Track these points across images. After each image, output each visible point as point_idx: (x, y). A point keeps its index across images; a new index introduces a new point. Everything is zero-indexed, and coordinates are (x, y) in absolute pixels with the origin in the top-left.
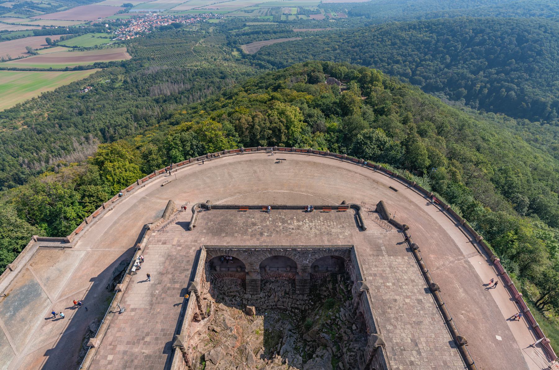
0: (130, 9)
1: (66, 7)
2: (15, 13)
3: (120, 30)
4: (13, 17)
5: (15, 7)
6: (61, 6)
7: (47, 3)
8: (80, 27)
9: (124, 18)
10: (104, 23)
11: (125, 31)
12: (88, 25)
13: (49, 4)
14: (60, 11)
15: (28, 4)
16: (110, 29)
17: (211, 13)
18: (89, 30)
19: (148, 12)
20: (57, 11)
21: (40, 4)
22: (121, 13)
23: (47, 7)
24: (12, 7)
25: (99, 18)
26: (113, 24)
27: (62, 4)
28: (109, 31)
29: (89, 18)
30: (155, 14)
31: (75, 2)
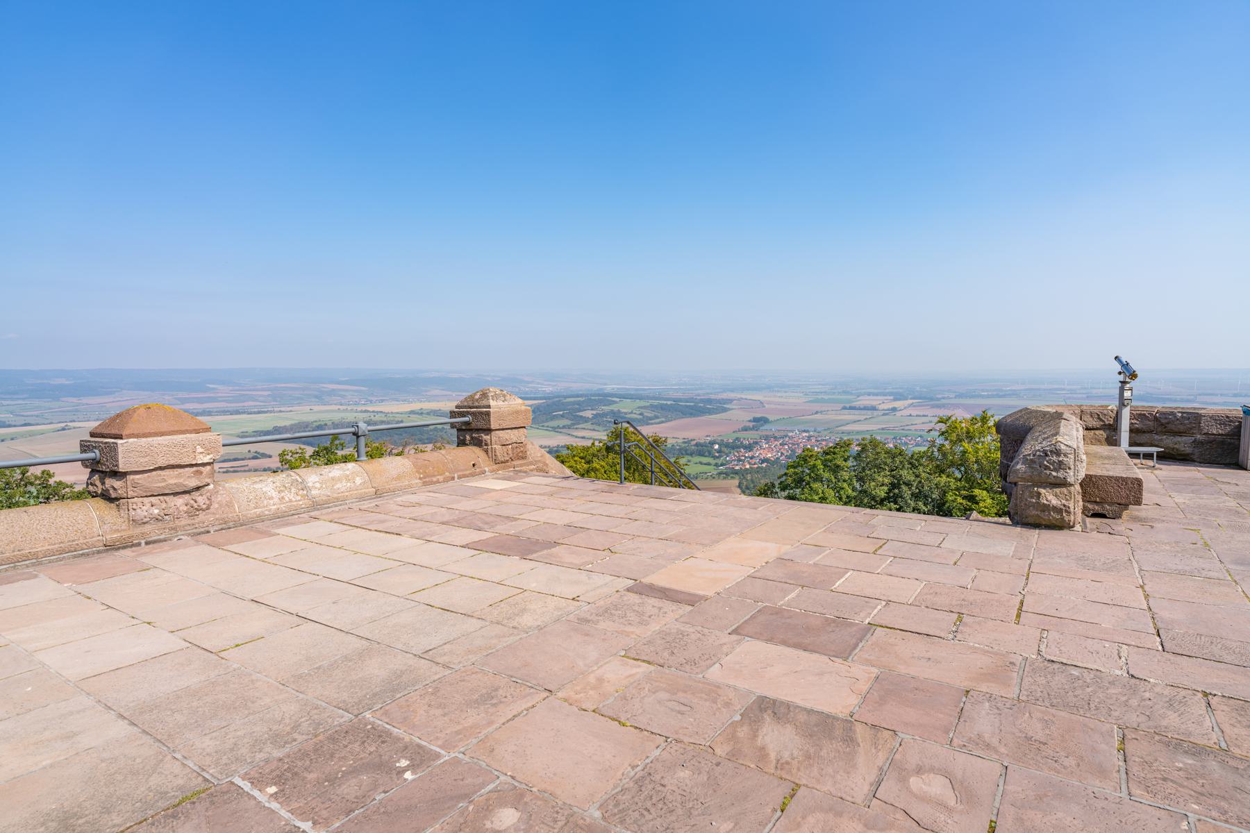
0: (762, 425)
1: (663, 419)
2: (592, 424)
3: (736, 454)
4: (588, 429)
5: (595, 416)
6: (657, 417)
7: (638, 412)
8: (673, 445)
9: (748, 437)
10: (712, 443)
11: (745, 456)
12: (687, 445)
13: (641, 414)
14: (652, 424)
15: (614, 413)
16: (719, 451)
17: (921, 436)
18: (686, 451)
19: (792, 431)
20: (648, 424)
21: (630, 413)
22: (746, 430)
23: (637, 419)
24: (591, 416)
25: (707, 436)
26: (727, 445)
27: (659, 414)
28: (717, 454)
29: (690, 435)
30: (804, 434)
31: (680, 413)
